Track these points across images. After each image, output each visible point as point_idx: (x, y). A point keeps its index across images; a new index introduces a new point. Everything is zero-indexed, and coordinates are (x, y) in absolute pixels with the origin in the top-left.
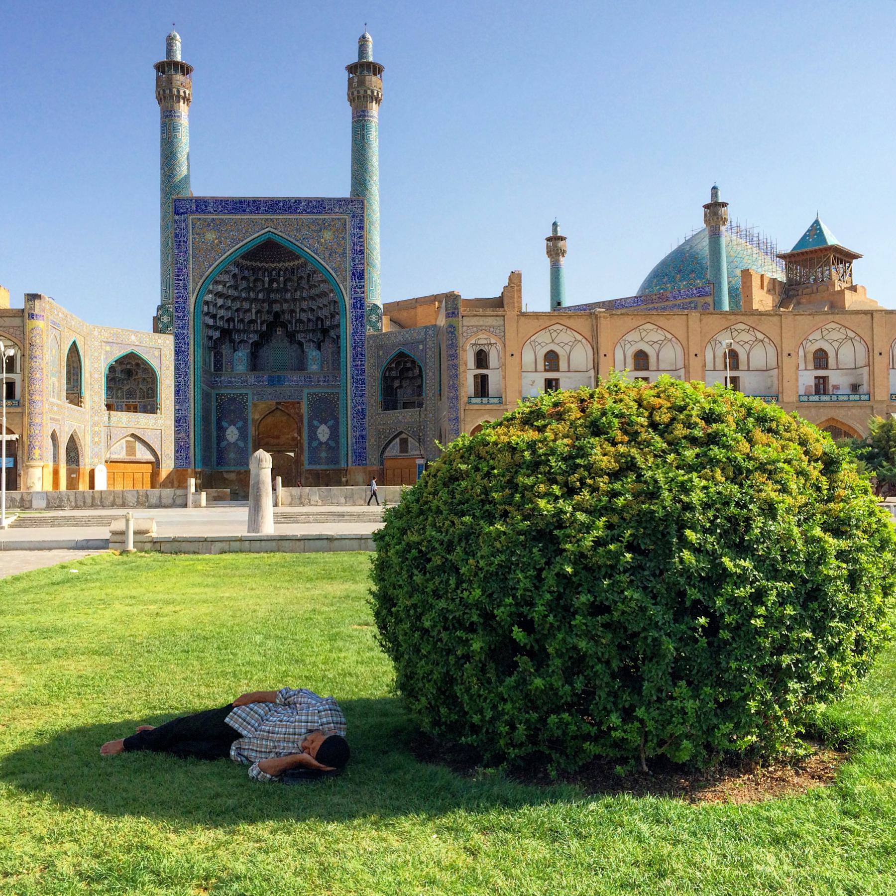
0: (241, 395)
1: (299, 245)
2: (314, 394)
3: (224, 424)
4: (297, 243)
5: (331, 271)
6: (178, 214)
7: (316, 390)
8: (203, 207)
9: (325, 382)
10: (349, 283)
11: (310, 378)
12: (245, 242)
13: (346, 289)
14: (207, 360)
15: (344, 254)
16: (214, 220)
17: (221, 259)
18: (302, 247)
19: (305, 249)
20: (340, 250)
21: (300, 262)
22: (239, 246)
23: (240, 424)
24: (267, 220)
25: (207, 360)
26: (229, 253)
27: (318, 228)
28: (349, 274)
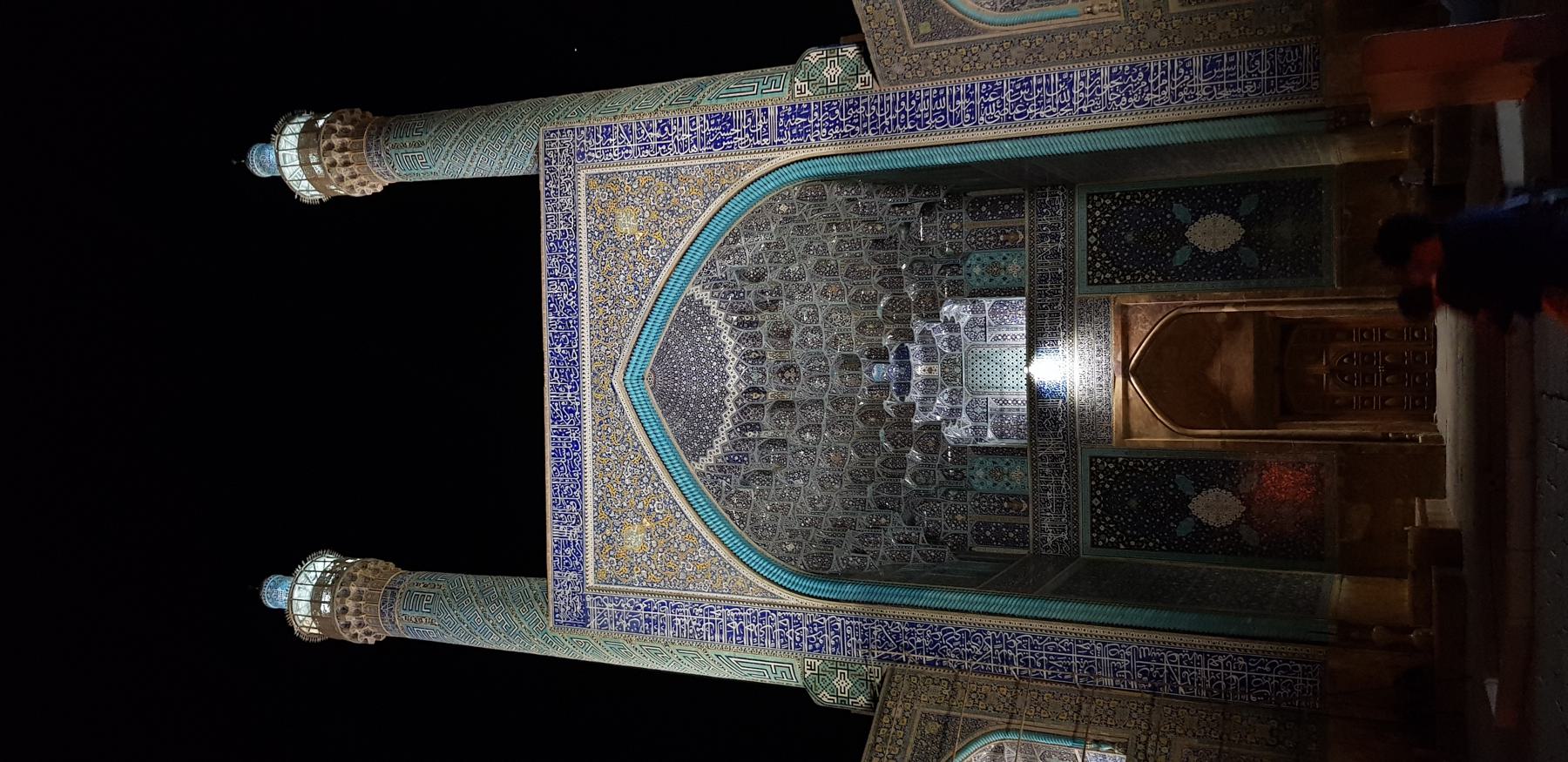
0: (1093, 475)
1: (651, 298)
2: (1090, 266)
3: (1184, 529)
4: (647, 306)
5: (713, 207)
6: (586, 619)
7: (1081, 257)
8: (569, 551)
9: (1055, 238)
10: (740, 157)
11: (1043, 279)
12: (648, 448)
13: (758, 162)
14: (982, 567)
15: (668, 175)
16: (597, 527)
17: (689, 512)
18: (655, 290)
19: (660, 282)
20: (661, 186)
21: (705, 296)
22: (656, 464)
23: (1184, 483)
24: (594, 386)
25: (982, 567)
26: (674, 492)
27: (610, 248)
28: (720, 158)
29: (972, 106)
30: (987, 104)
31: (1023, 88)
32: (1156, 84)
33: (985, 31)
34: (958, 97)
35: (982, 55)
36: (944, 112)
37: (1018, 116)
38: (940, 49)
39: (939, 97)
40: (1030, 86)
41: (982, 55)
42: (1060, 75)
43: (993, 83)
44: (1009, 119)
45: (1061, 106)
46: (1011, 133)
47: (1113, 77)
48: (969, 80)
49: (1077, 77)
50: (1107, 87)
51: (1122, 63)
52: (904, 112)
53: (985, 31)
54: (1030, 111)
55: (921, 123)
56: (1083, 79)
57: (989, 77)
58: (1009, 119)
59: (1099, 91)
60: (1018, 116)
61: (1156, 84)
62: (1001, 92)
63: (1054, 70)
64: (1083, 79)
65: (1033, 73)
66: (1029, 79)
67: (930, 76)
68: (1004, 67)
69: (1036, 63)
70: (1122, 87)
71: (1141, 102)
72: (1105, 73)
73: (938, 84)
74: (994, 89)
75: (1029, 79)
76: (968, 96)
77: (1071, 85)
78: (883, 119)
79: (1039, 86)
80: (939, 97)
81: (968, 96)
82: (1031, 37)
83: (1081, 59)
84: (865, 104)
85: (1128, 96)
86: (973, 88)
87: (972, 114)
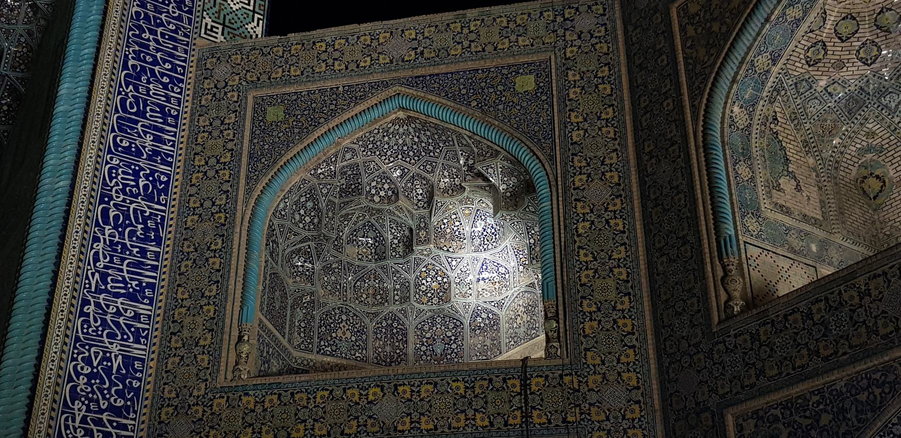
29: (139, 154)
30: (136, 174)
31: (146, 229)
32: (99, 422)
33: (249, 192)
34: (157, 139)
35: (214, 183)
36: (143, 114)
37: (105, 212)
38: (238, 128)
39: (165, 114)
40: (146, 239)
41: (214, 183)
42: (151, 286)
43: (165, 191)
44: (105, 198)
45: (104, 277)
46: (81, 195)
47: (128, 361)
48: (179, 161)
49: (143, 309)
50: (115, 349)
51: (147, 380)
52: (155, 62)
53: (249, 192)
54: (108, 230)
55: (134, 78)
56: (137, 317)
57: (176, 190)
58: (105, 198)
59: (112, 336)
60: (105, 212)
61: (99, 422)
62: (149, 198)
63: (163, 279)
64: (137, 317)
65: (167, 250)
66: (158, 241)
67: (199, 111)
68: (185, 209)
69: (180, 255)
70: (108, 371)
71: (74, 395)
72: (137, 350)
73: (185, 121)
74: (157, 190)
75: (158, 241)
76: (156, 153)
77: (132, 297)
78: (152, 32)
79: (143, 252)
80: (165, 114)
81: (156, 153)
82: (225, 252)
83: (170, 318)
84: (179, 18)
85: (90, 376)
86: (164, 162)
87: (127, 150)
